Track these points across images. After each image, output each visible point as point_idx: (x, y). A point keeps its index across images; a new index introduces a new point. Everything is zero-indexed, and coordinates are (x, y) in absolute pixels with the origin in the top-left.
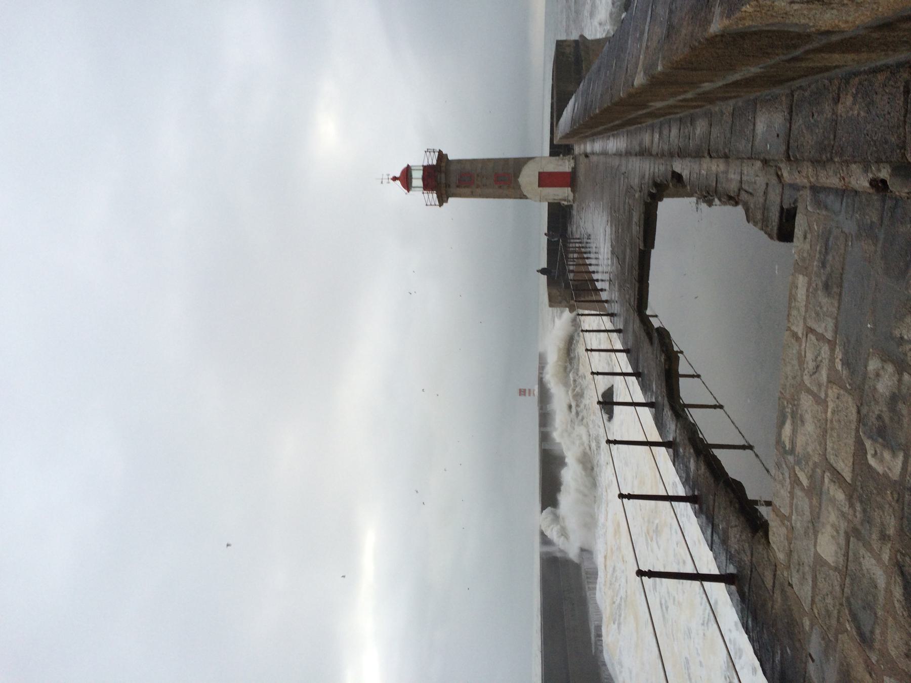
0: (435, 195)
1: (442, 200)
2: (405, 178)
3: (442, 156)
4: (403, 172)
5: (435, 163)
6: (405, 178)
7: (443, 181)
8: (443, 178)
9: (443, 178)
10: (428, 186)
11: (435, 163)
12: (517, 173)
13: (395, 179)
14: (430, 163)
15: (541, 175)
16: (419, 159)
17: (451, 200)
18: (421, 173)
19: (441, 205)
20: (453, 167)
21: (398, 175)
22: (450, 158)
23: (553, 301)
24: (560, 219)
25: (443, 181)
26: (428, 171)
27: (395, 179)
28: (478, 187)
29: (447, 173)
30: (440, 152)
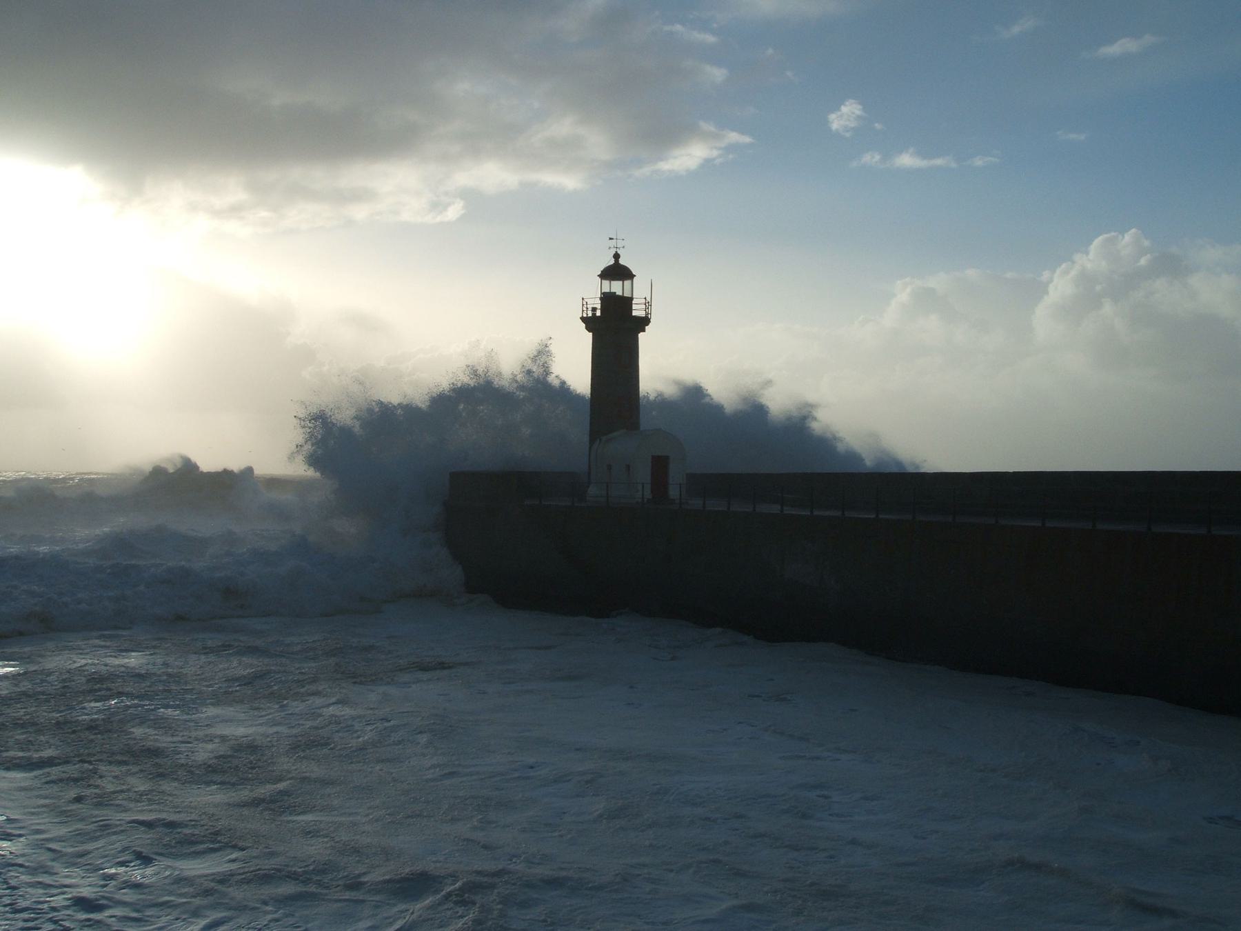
1: (590, 323)
2: (617, 271)
3: (644, 322)
5: (634, 313)
6: (617, 271)
11: (634, 313)
13: (617, 256)
14: (634, 307)
16: (639, 292)
19: (583, 319)
21: (622, 261)
22: (641, 335)
26: (627, 302)
27: (617, 256)
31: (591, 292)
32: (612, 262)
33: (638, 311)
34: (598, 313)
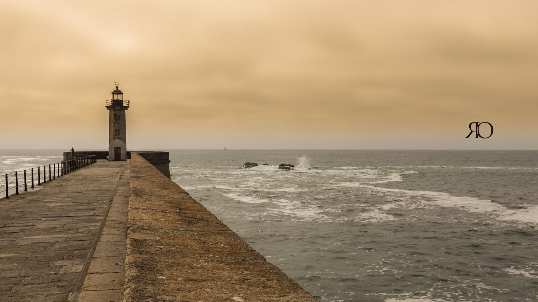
0: (111, 105)
2: (117, 92)
3: (127, 108)
4: (120, 91)
6: (117, 92)
7: (117, 108)
8: (118, 109)
9: (118, 109)
12: (119, 138)
13: (117, 87)
15: (120, 148)
20: (122, 112)
23: (66, 155)
24: (102, 155)
25: (117, 108)
27: (117, 87)
28: (114, 122)
29: (120, 110)
30: (128, 107)
31: (109, 98)
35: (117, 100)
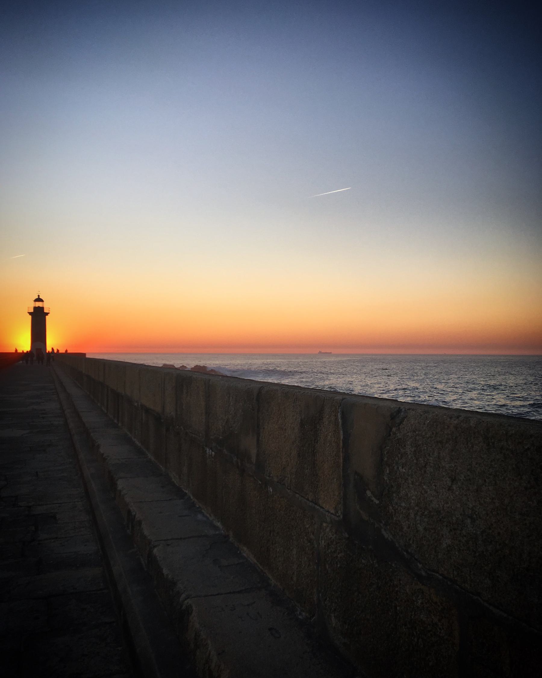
0: (32, 311)
1: (30, 313)
2: (39, 300)
5: (45, 311)
6: (39, 300)
10: (35, 308)
11: (45, 311)
13: (39, 296)
16: (47, 306)
17: (30, 317)
18: (41, 306)
19: (29, 313)
21: (40, 297)
22: (47, 317)
26: (43, 308)
27: (39, 296)
31: (31, 305)
32: (37, 297)
33: (46, 311)
34: (32, 311)
35: (39, 307)
